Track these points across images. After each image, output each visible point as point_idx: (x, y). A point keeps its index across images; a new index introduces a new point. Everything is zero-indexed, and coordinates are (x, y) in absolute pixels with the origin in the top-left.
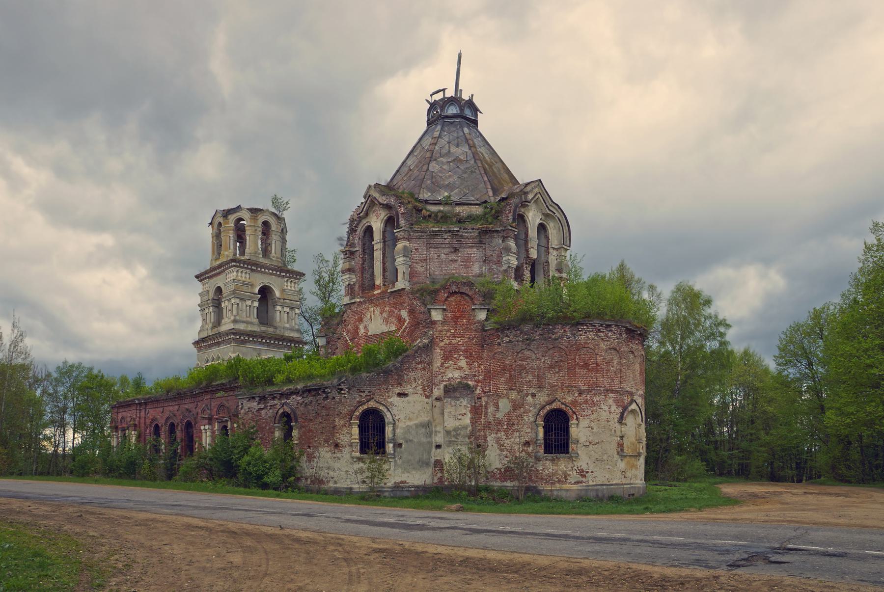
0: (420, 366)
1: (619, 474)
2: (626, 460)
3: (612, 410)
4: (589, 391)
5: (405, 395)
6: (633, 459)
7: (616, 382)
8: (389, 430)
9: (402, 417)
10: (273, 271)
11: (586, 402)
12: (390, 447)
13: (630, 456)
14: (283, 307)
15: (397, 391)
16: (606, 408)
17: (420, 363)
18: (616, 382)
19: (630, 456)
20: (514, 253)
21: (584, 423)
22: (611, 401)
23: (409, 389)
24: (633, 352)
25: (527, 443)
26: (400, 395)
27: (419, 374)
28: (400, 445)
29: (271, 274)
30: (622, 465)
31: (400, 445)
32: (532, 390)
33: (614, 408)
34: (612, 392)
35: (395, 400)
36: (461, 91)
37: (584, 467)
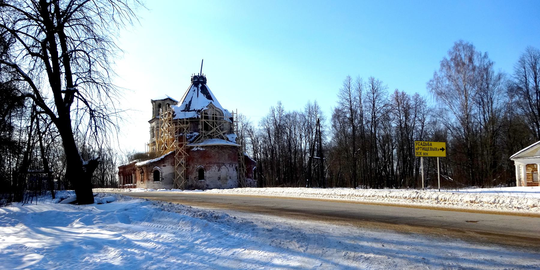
3: (216, 168)
4: (209, 163)
5: (165, 166)
8: (160, 174)
9: (164, 171)
11: (208, 166)
12: (160, 179)
15: (163, 165)
16: (214, 168)
21: (208, 172)
22: (215, 166)
23: (166, 164)
25: (195, 178)
26: (164, 166)
27: (170, 160)
28: (164, 179)
31: (164, 179)
32: (196, 164)
33: (217, 167)
35: (162, 167)
37: (208, 184)
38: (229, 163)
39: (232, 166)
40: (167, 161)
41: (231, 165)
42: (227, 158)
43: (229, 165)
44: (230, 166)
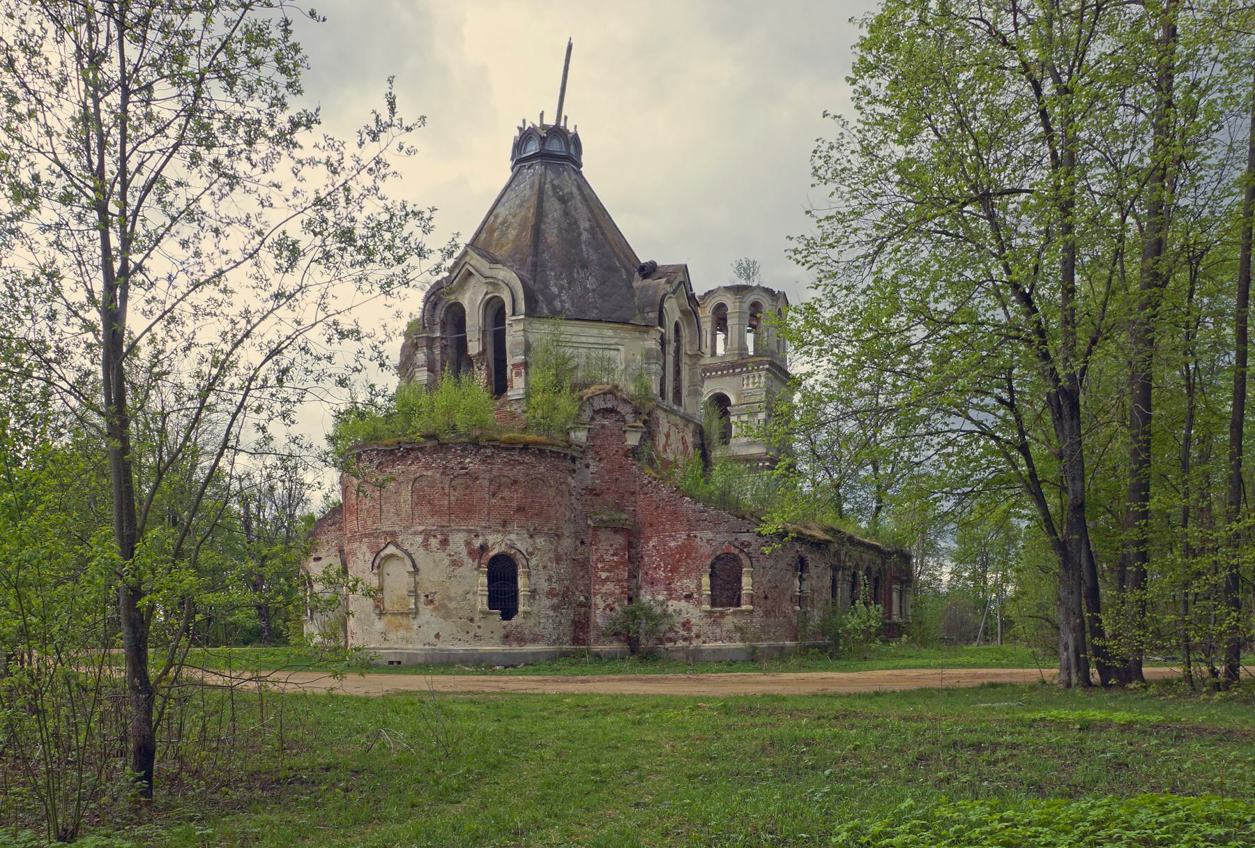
0: (333, 527)
1: (378, 637)
2: (385, 619)
3: (367, 559)
6: (399, 617)
7: (369, 523)
10: (722, 371)
13: (393, 614)
14: (739, 416)
17: (334, 523)
18: (369, 523)
19: (393, 614)
20: (422, 366)
22: (364, 548)
24: (393, 479)
29: (722, 375)
30: (380, 625)
34: (366, 535)
36: (566, 118)
38: (421, 528)
39: (445, 542)
40: (324, 537)
41: (434, 542)
42: (406, 508)
43: (420, 539)
44: (426, 545)
